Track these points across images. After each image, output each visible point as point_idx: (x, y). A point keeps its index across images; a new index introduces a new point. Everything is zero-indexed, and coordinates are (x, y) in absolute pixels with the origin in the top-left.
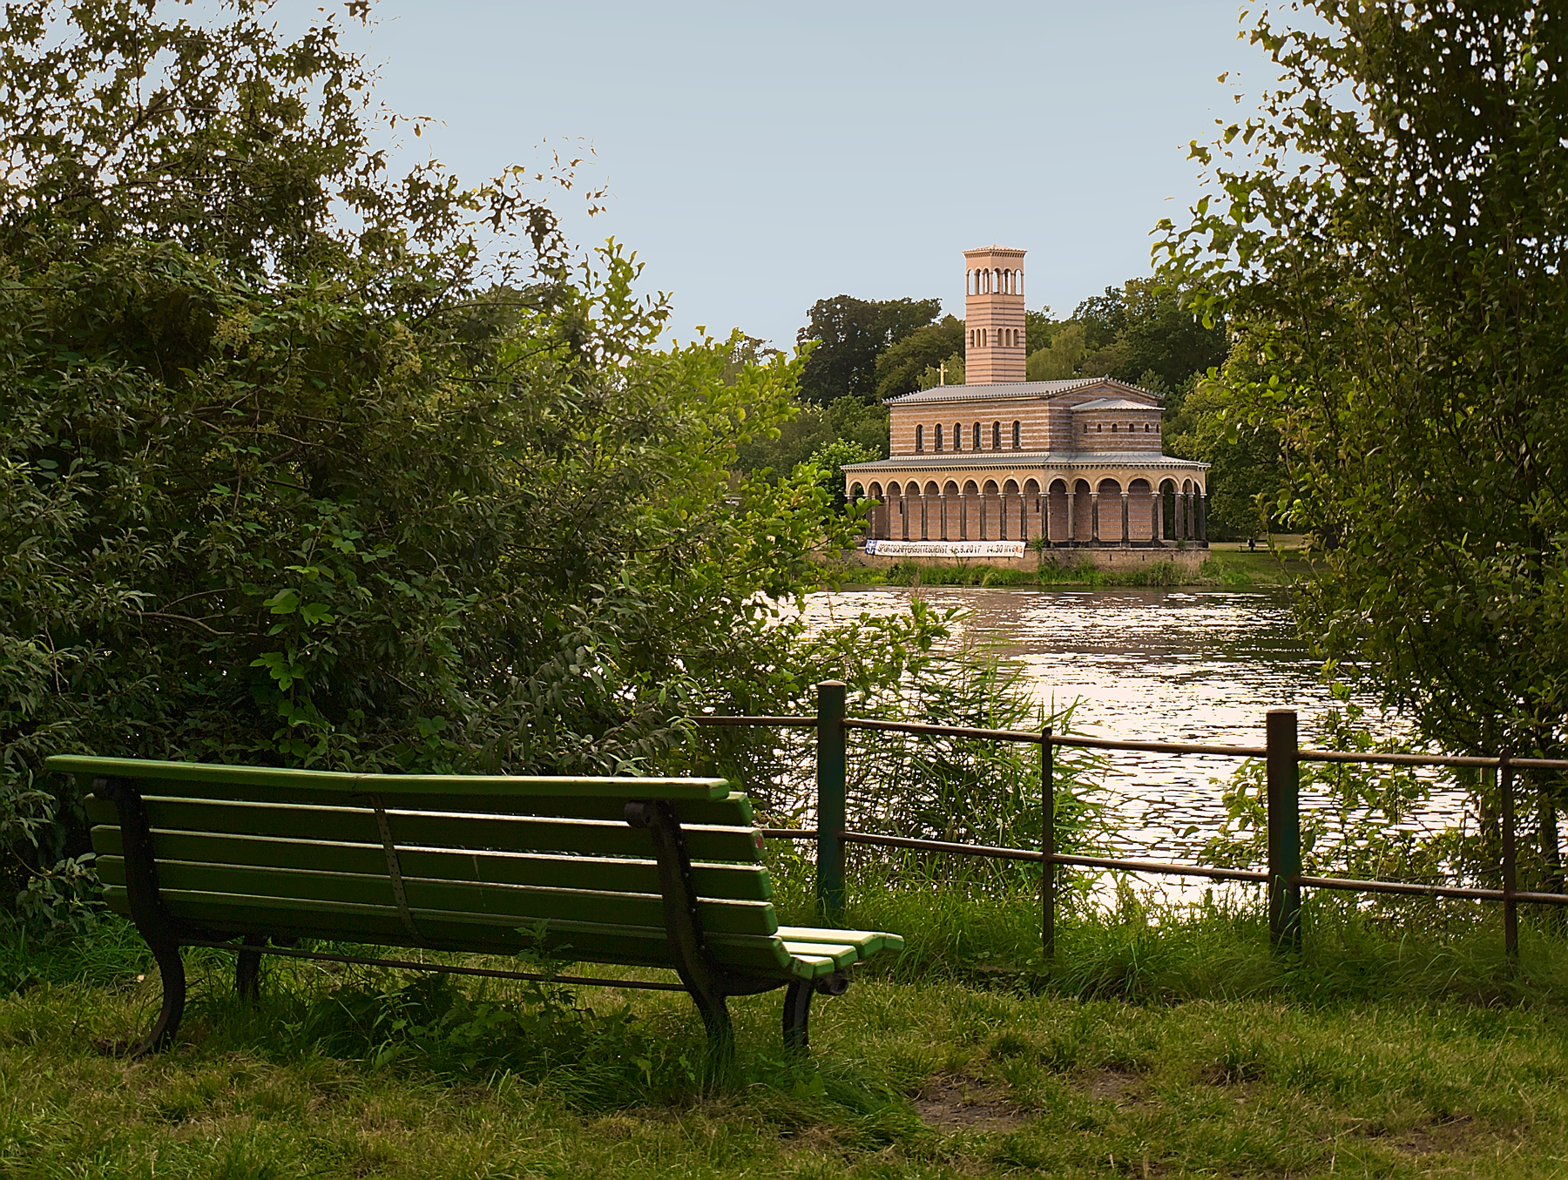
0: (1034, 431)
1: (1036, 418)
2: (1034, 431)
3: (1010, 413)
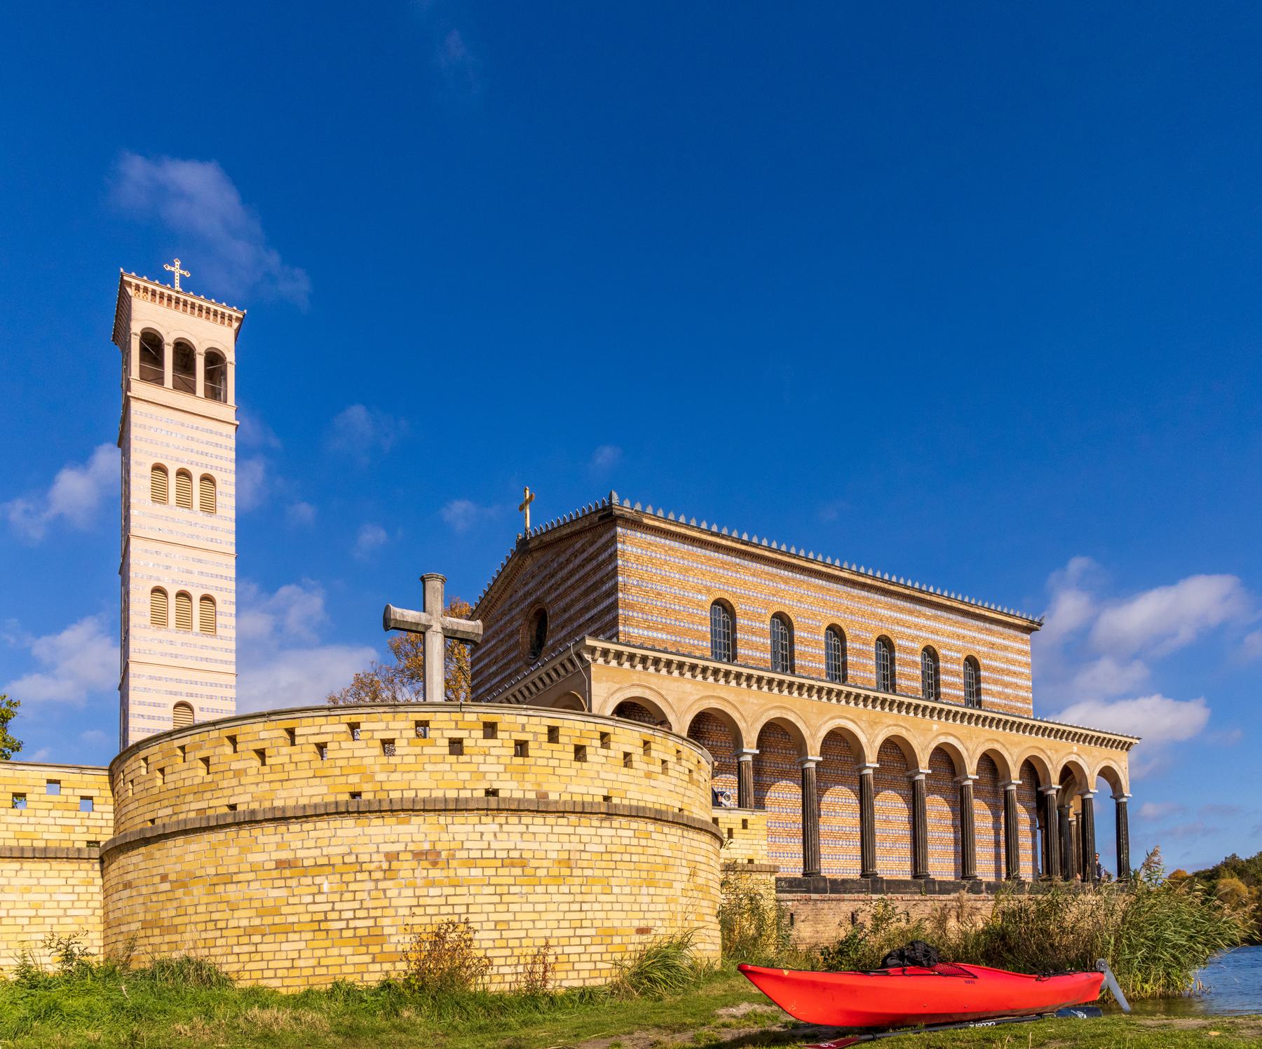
0: (1006, 685)
1: (1008, 661)
2: (1006, 685)
3: (958, 637)
